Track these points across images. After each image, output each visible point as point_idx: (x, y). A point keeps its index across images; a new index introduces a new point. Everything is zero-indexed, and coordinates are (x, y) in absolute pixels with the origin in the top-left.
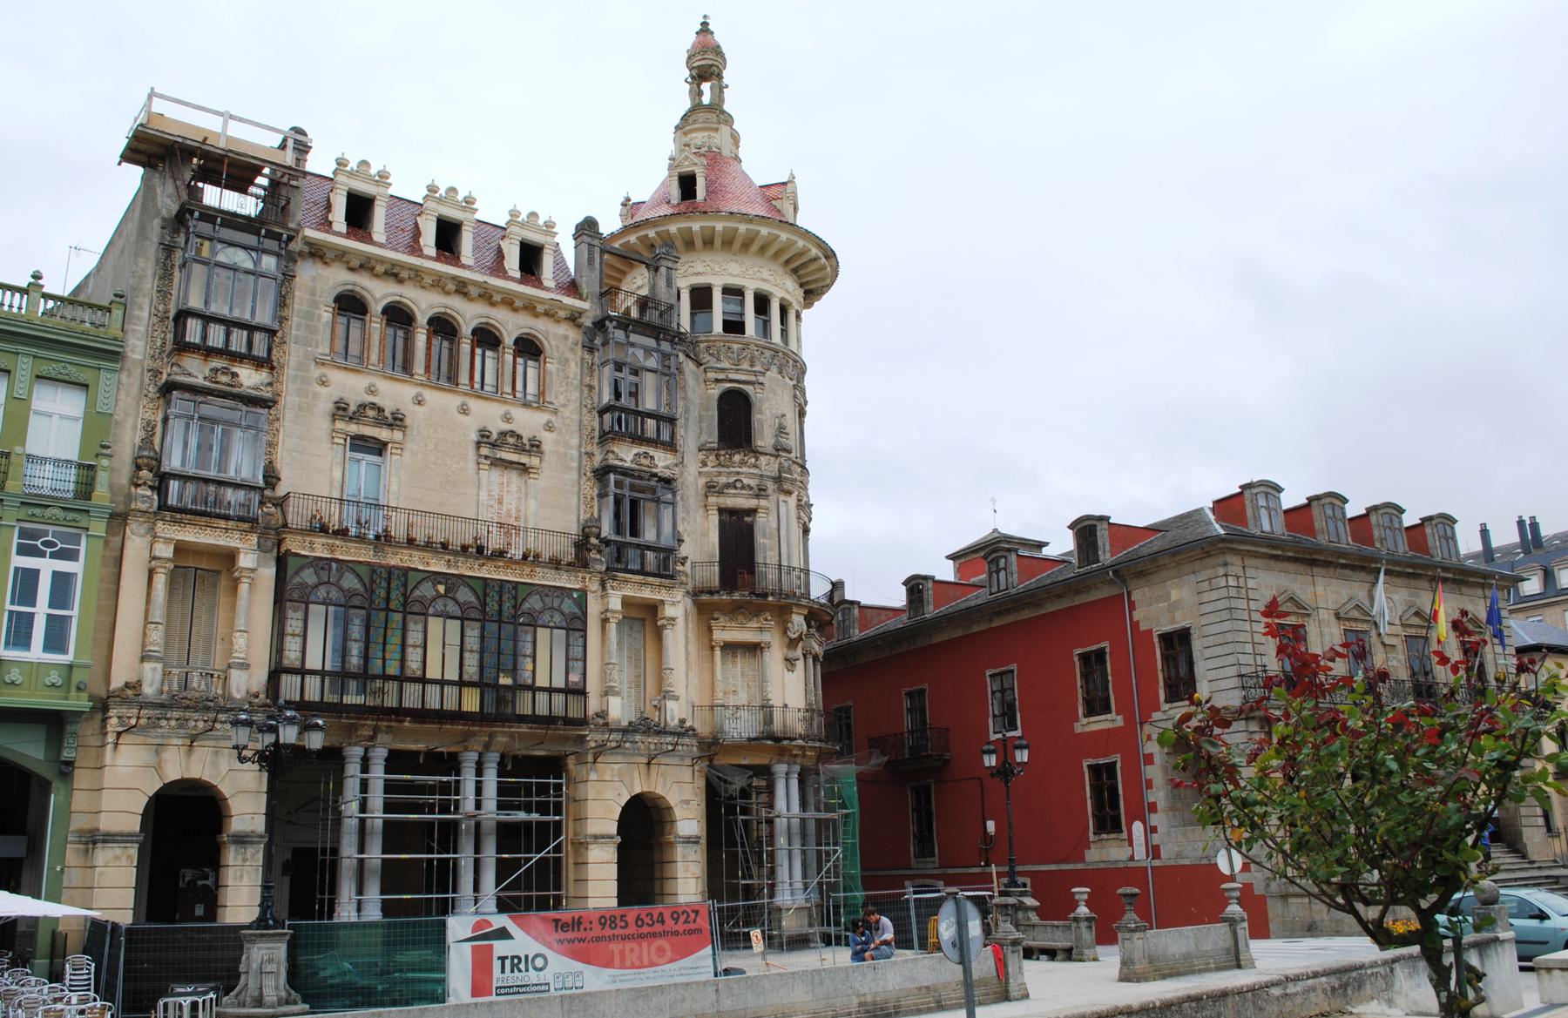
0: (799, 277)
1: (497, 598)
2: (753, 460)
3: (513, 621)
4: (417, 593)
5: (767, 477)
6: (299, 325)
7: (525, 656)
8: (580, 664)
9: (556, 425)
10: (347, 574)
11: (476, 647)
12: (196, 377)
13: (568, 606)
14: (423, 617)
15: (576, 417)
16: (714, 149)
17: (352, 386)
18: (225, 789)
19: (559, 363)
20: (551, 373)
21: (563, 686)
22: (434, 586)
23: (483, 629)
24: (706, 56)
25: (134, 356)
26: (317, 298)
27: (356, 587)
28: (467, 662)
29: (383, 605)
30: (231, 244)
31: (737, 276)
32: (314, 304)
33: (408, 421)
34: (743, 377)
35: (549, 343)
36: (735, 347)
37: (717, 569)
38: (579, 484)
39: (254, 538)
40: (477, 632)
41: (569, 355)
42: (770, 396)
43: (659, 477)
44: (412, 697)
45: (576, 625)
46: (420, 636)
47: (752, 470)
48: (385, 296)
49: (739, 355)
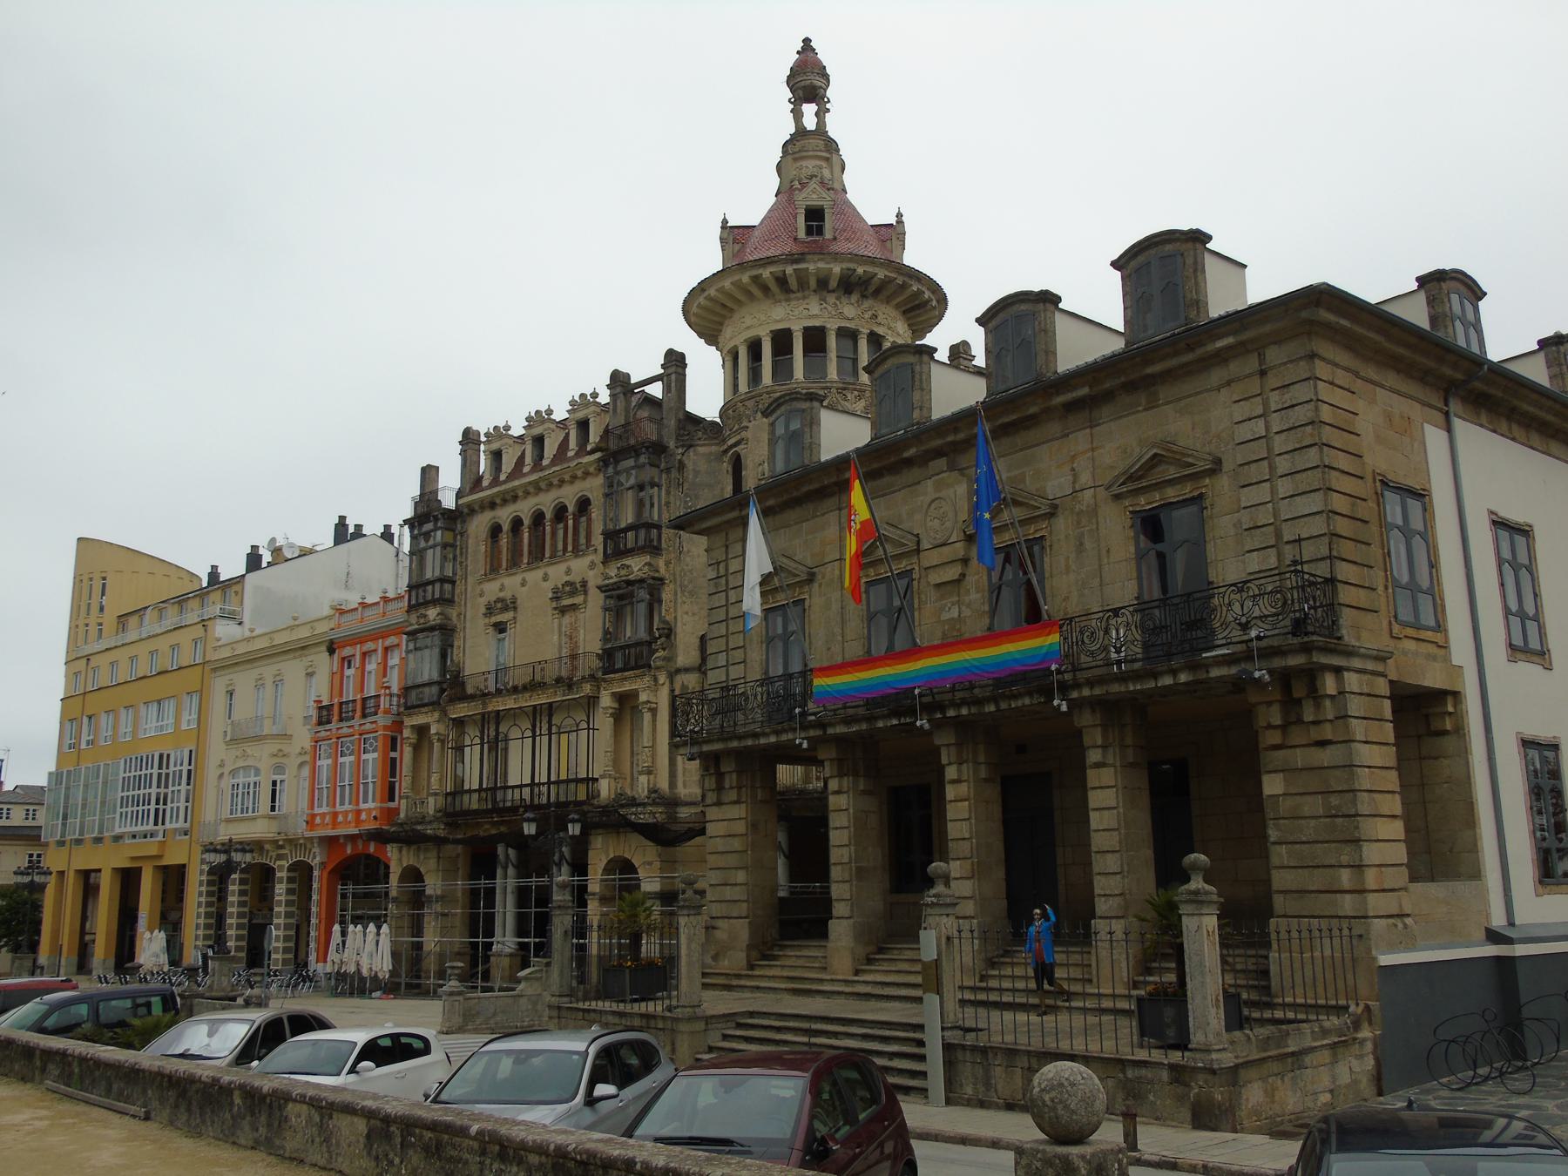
17: (492, 590)
39: (436, 715)
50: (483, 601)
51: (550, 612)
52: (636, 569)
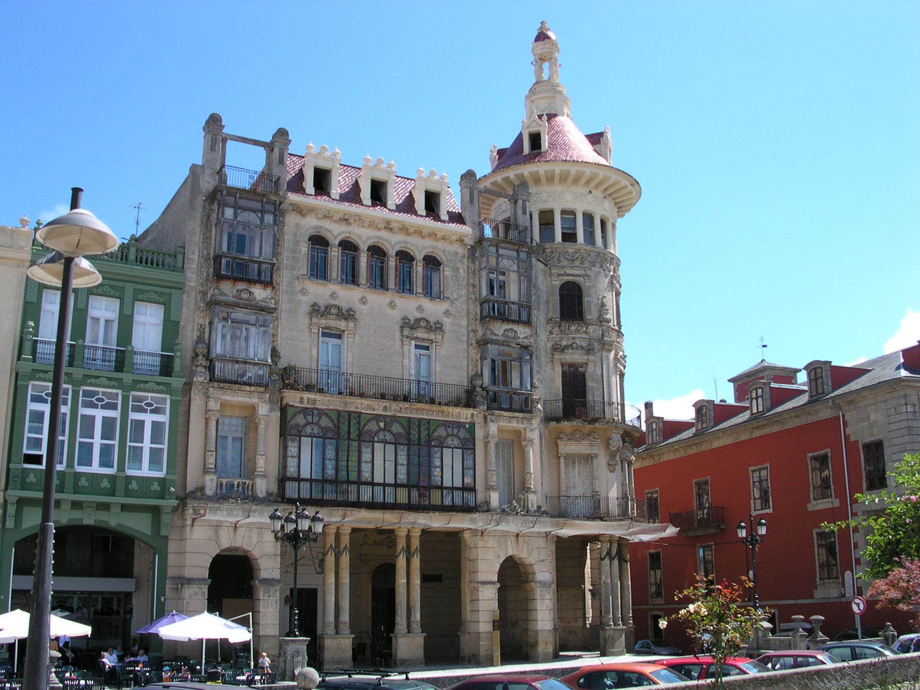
0: (614, 199)
1: (417, 430)
2: (584, 329)
3: (427, 444)
4: (367, 428)
6: (288, 257)
7: (436, 467)
8: (472, 471)
9: (452, 313)
10: (323, 417)
11: (405, 462)
12: (229, 296)
13: (463, 434)
14: (371, 444)
15: (465, 307)
18: (256, 553)
19: (453, 271)
20: (447, 277)
21: (461, 486)
22: (378, 423)
23: (409, 450)
25: (190, 284)
26: (298, 239)
27: (329, 425)
28: (399, 472)
29: (346, 436)
30: (245, 209)
32: (297, 243)
33: (357, 316)
34: (576, 272)
35: (446, 258)
36: (570, 251)
37: (561, 405)
38: (468, 351)
40: (405, 453)
41: (459, 265)
43: (521, 345)
44: (366, 494)
45: (468, 445)
46: (370, 455)
48: (340, 234)
49: (573, 257)
50: (306, 302)
51: (398, 335)
52: (522, 336)
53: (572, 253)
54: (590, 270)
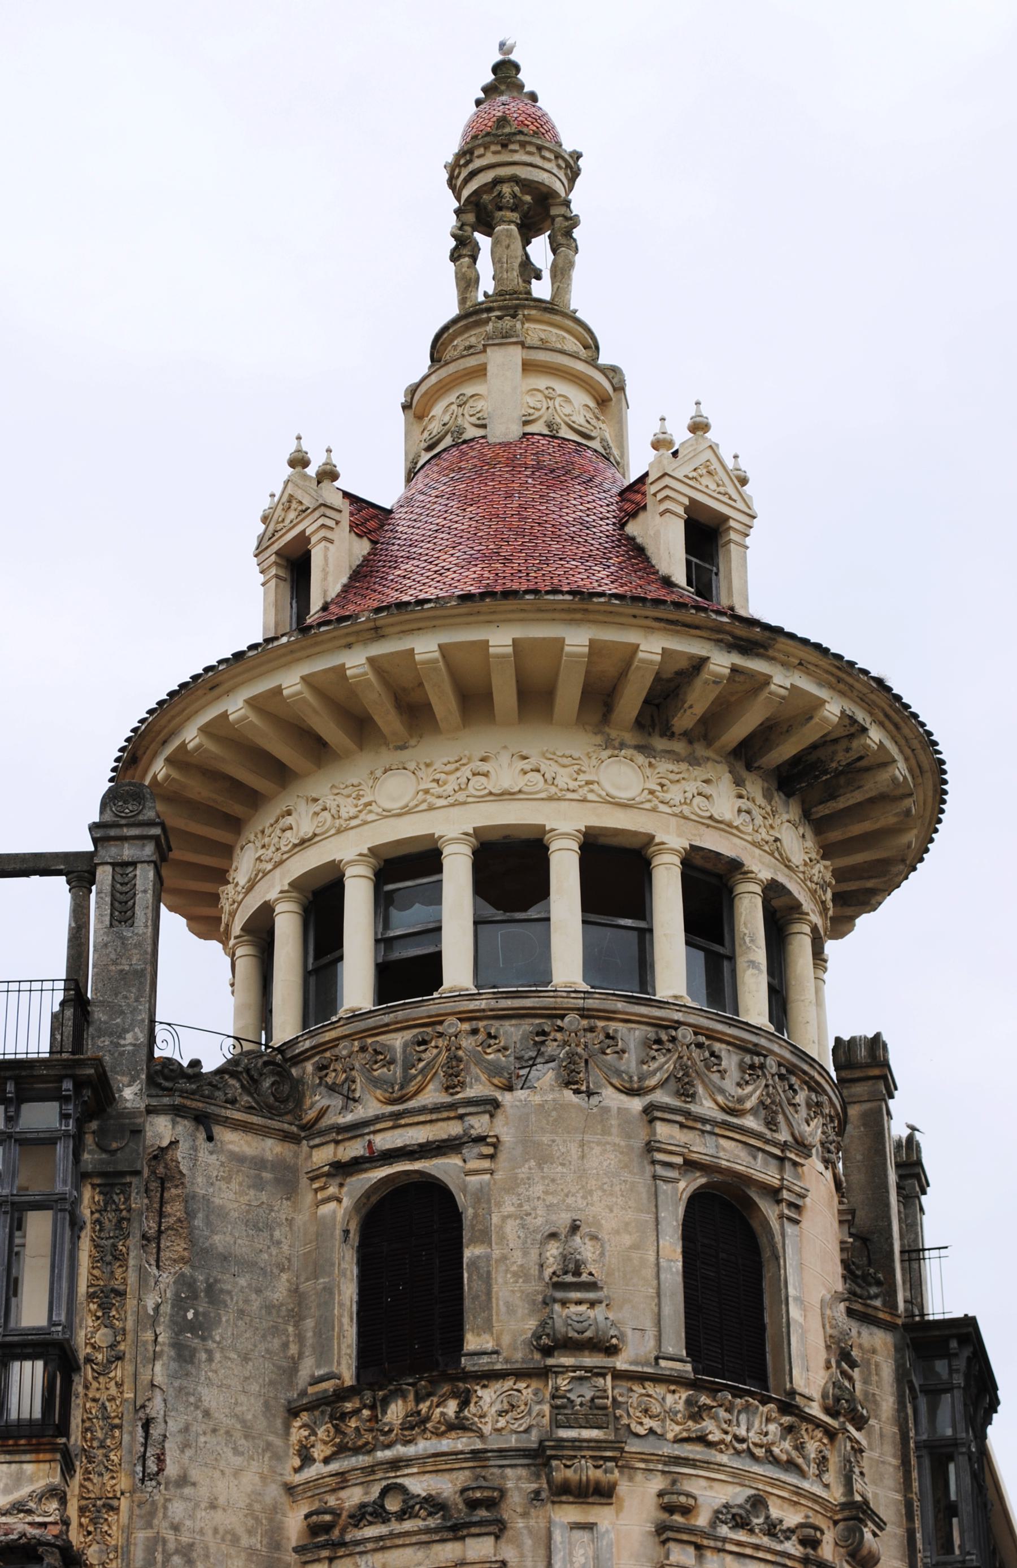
2: (451, 1407)
5: (502, 1453)
16: (471, 432)
24: (477, 163)
31: (406, 812)
42: (523, 1172)
47: (446, 1444)
49: (408, 1065)
53: (405, 1045)
54: (491, 1106)
